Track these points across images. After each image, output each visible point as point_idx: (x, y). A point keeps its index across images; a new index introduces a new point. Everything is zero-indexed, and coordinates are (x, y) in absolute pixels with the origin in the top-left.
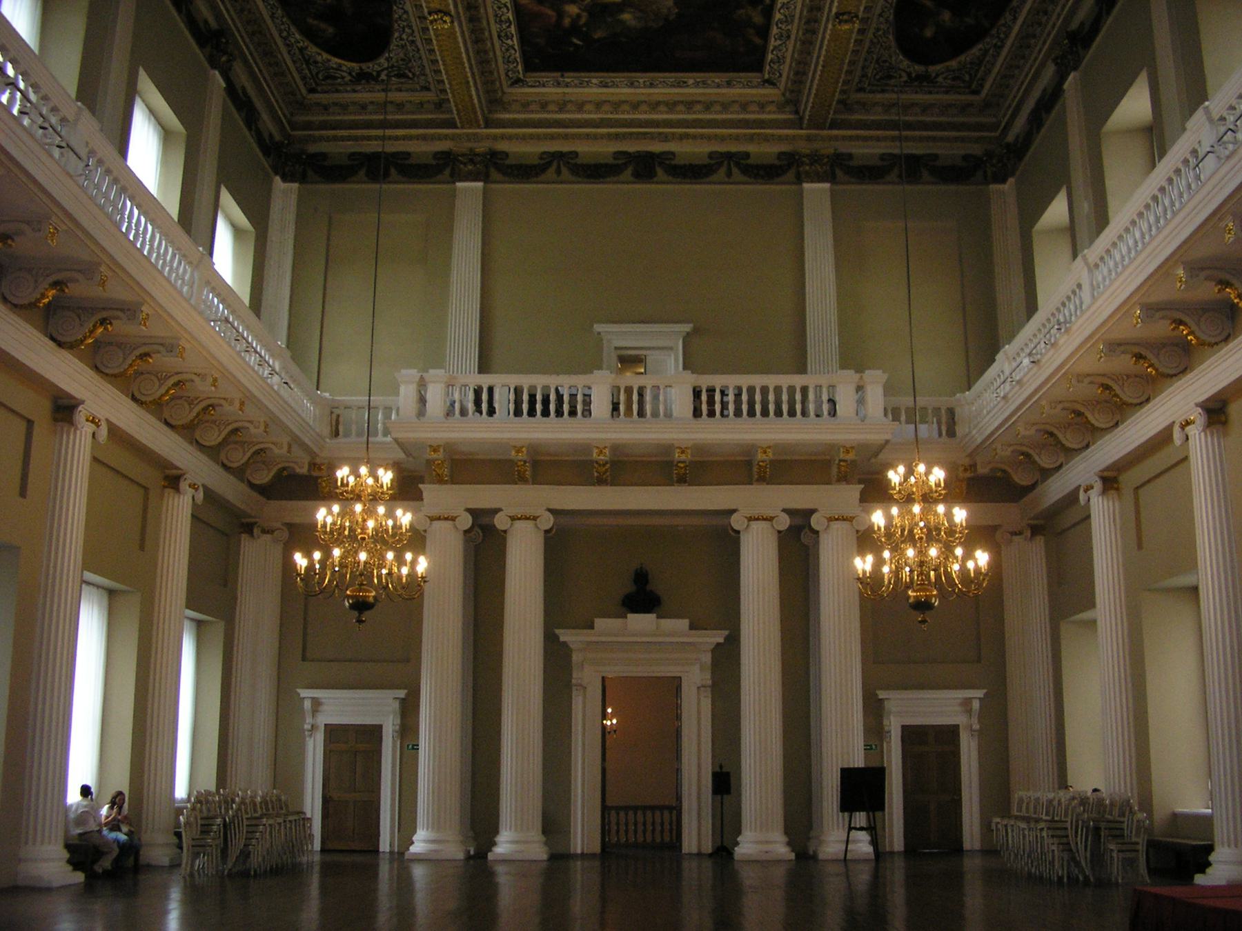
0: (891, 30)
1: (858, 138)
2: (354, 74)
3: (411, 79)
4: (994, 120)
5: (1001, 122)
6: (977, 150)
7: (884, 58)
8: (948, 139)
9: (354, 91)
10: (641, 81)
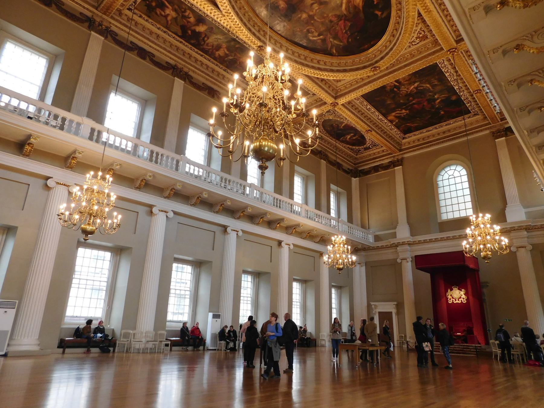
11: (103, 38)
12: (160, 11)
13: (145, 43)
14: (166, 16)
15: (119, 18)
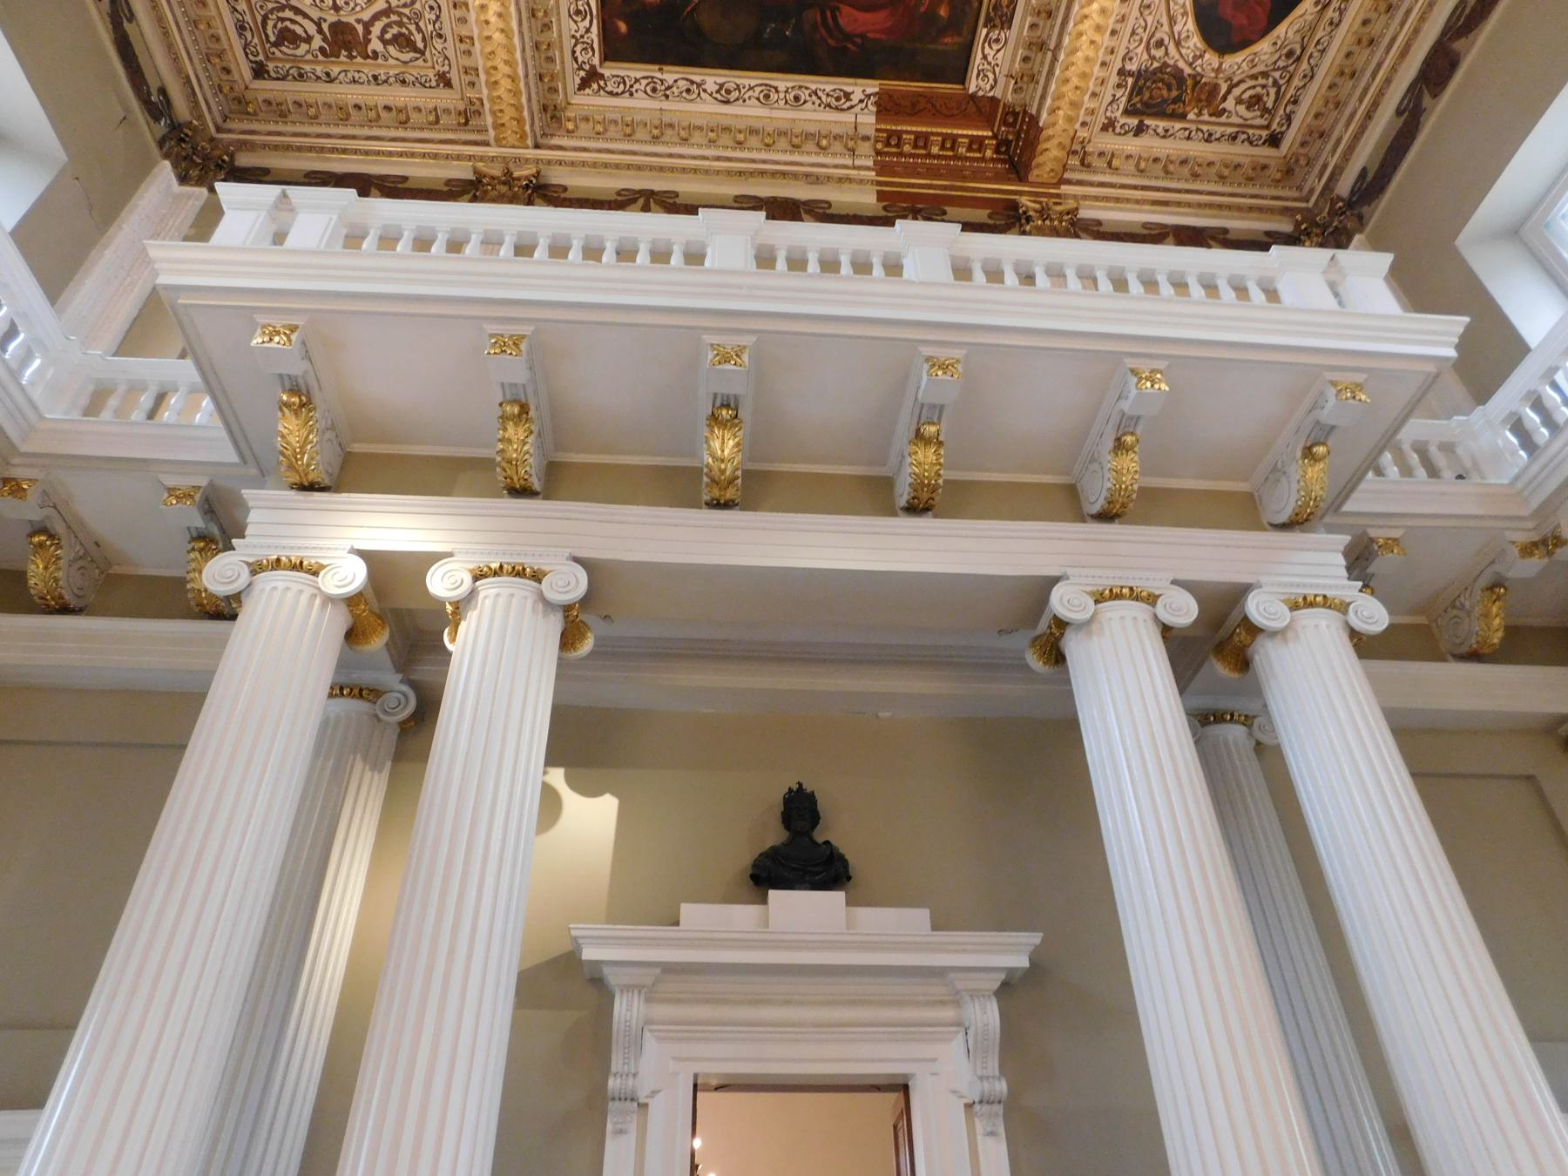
1: (1106, 199)
2: (325, 27)
4: (1295, 194)
5: (1312, 191)
7: (1158, 36)
8: (1239, 208)
9: (330, 79)
10: (782, 86)
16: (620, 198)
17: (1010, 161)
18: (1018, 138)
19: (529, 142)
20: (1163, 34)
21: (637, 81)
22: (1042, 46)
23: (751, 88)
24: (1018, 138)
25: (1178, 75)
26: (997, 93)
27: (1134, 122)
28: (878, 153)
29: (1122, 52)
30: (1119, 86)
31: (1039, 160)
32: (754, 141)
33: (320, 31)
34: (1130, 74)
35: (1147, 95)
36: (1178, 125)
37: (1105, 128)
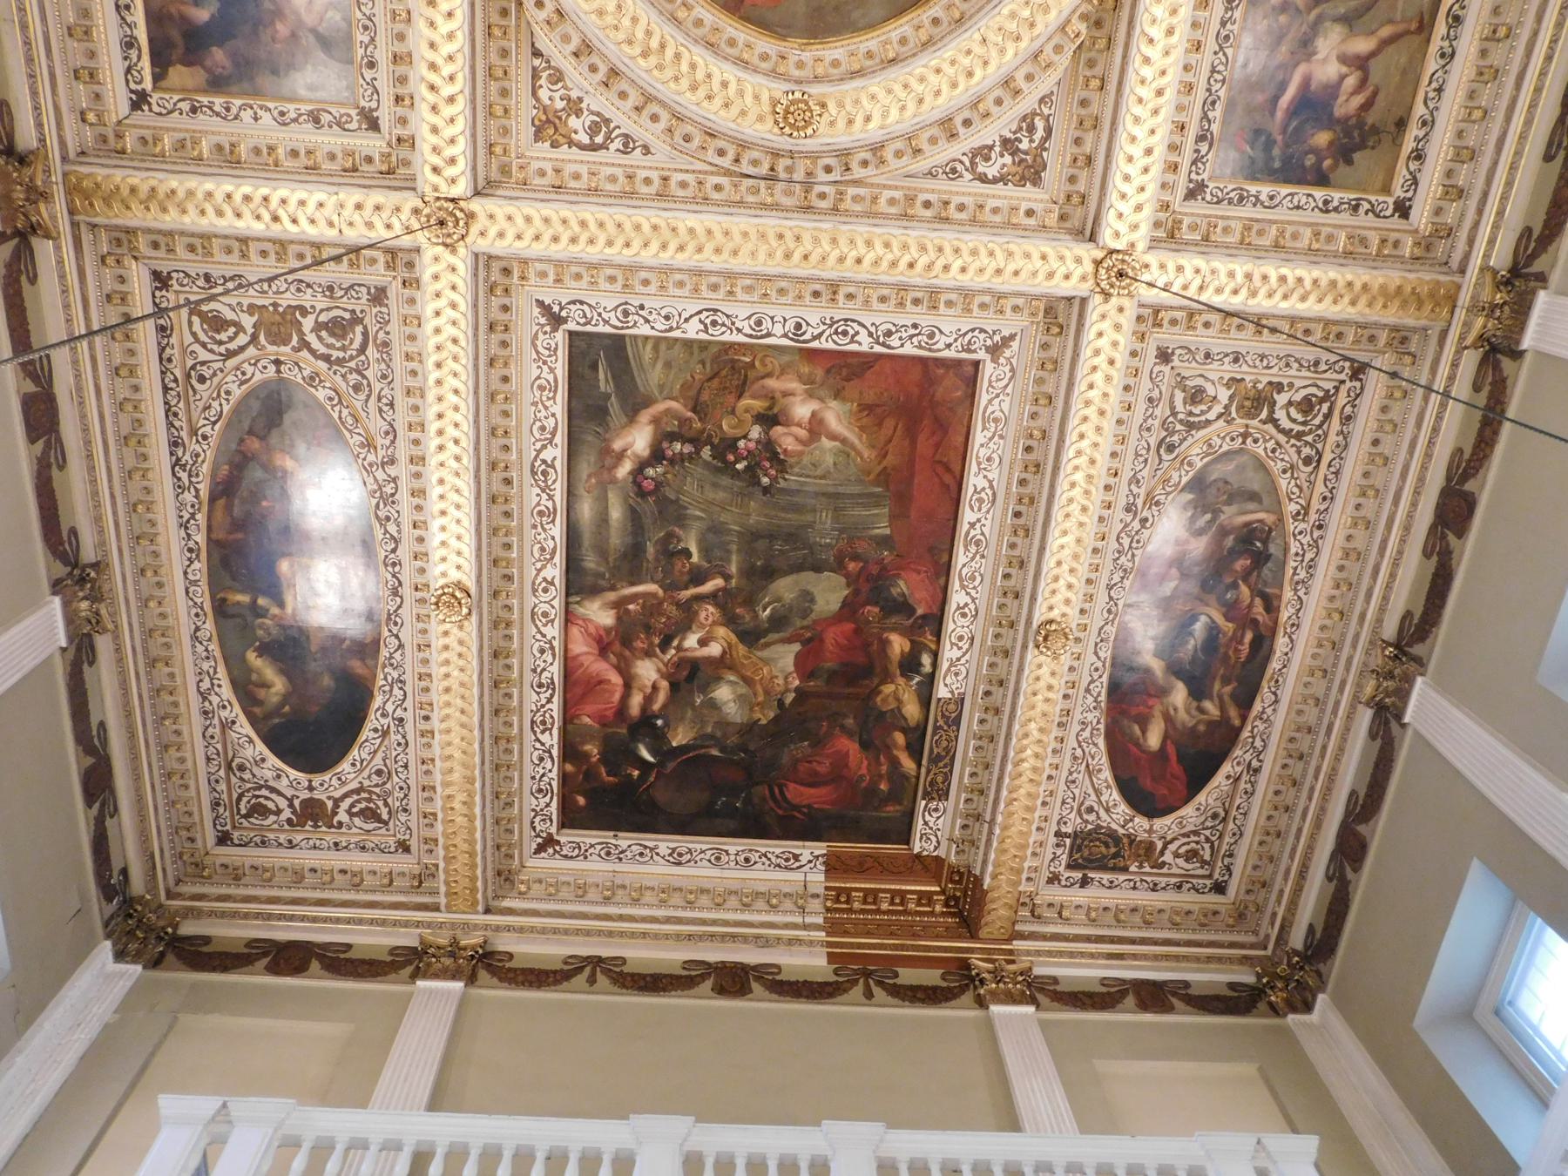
0: (1102, 727)
1: (1061, 954)
2: (297, 803)
3: (386, 823)
4: (1251, 939)
5: (1267, 936)
6: (1248, 978)
7: (1087, 804)
8: (1197, 959)
9: (291, 845)
11: (1542, 297)
12: (1342, 98)
13: (1538, 90)
14: (1361, 64)
15: (1463, 235)
16: (566, 968)
17: (959, 914)
18: (965, 895)
19: (480, 908)
20: (1091, 801)
21: (592, 846)
22: (978, 817)
23: (702, 852)
24: (965, 895)
25: (1112, 835)
26: (941, 853)
27: (1078, 875)
28: (828, 910)
29: (1056, 818)
30: (1058, 845)
31: (988, 918)
32: (704, 900)
33: (291, 805)
34: (1067, 835)
35: (1086, 853)
36: (1122, 877)
37: (1050, 881)
